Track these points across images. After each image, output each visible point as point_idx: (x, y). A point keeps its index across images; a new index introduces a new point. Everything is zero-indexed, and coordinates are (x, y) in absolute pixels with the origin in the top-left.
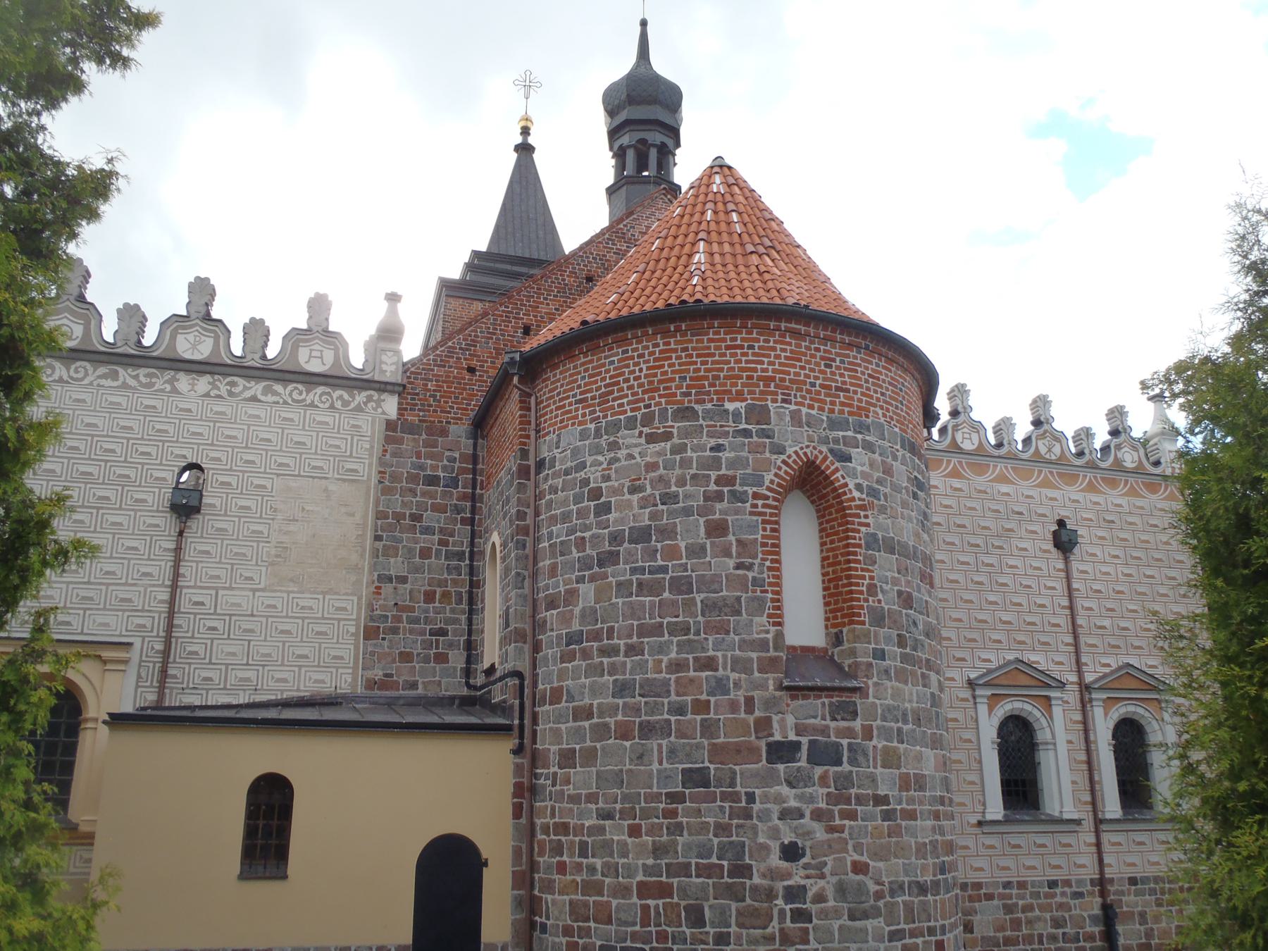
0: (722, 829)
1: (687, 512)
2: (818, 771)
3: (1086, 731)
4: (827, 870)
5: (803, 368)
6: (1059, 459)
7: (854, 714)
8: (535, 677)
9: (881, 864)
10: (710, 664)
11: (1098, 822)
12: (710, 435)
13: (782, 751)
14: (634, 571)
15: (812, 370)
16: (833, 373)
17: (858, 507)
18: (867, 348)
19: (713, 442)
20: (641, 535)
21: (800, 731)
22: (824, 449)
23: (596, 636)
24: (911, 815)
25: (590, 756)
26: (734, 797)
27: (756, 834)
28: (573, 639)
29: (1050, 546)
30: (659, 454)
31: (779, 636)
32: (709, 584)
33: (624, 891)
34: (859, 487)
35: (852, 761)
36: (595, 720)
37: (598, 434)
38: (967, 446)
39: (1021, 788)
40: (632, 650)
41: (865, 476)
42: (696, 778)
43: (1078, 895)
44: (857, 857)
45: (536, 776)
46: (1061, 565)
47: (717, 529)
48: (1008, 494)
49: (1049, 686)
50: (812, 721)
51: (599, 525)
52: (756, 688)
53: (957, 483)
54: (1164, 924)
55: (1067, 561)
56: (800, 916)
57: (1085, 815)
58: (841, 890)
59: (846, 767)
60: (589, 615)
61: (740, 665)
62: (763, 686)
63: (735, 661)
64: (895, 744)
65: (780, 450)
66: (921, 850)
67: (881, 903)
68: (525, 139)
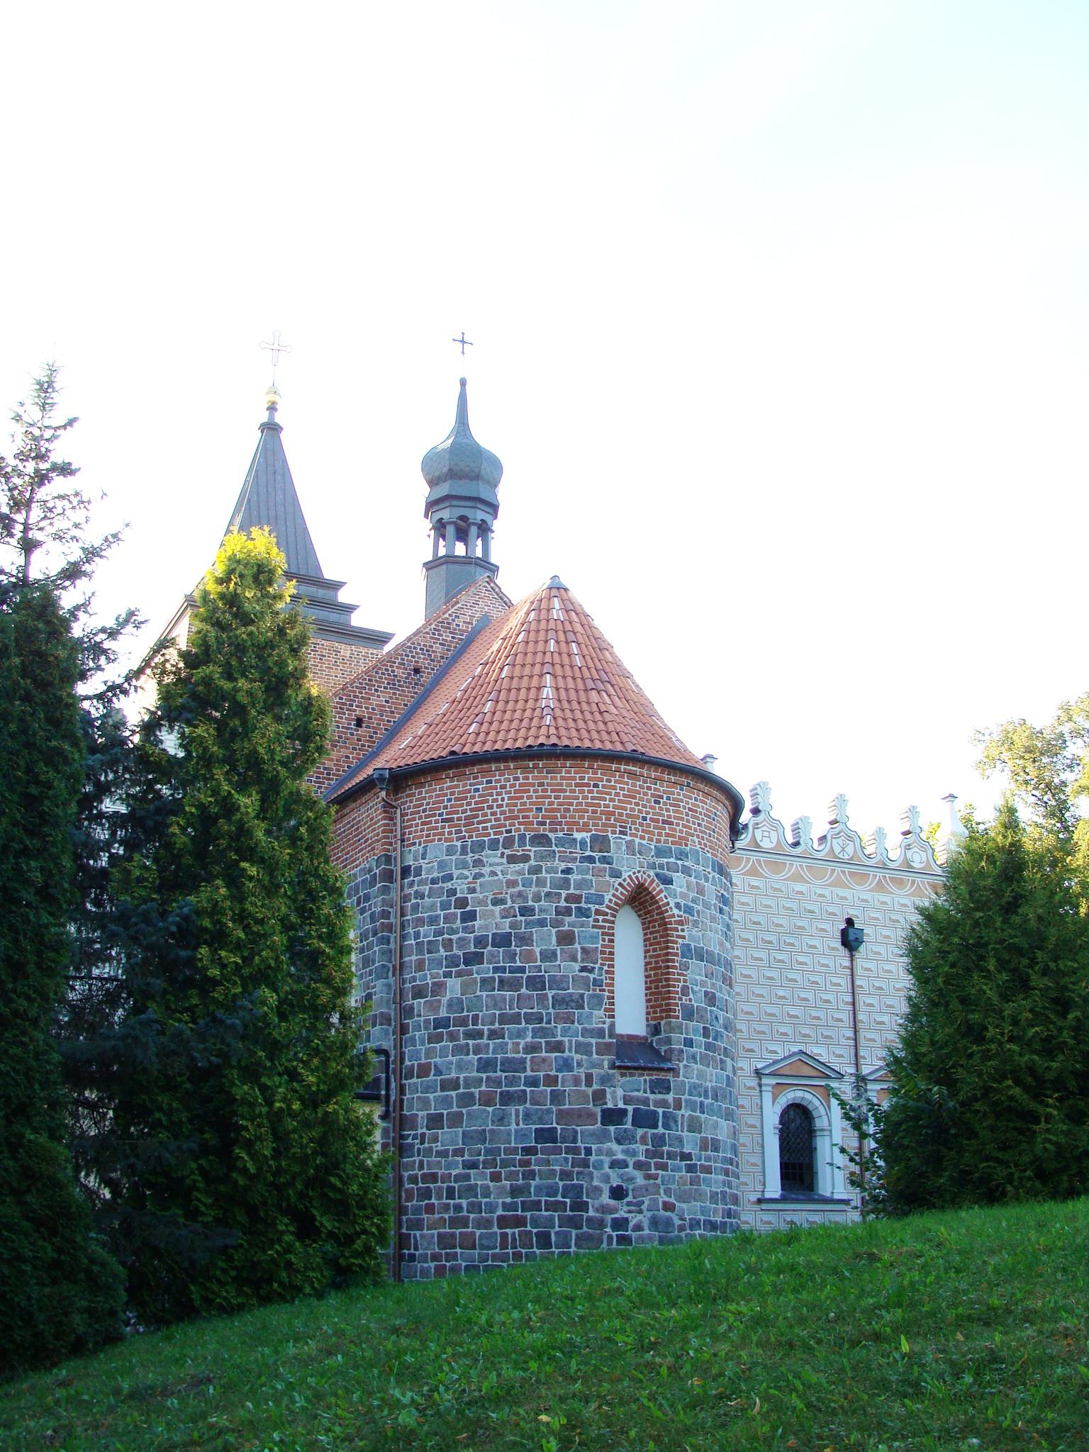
0: (565, 1175)
1: (542, 923)
2: (640, 1132)
4: (644, 1207)
5: (637, 804)
6: (851, 859)
7: (668, 1090)
8: (402, 1054)
9: (684, 1206)
10: (558, 1047)
12: (562, 859)
13: (613, 1116)
14: (496, 970)
15: (645, 806)
16: (661, 809)
18: (688, 785)
19: (563, 866)
20: (502, 940)
21: (627, 1100)
22: (652, 873)
23: (463, 1022)
24: (707, 1170)
25: (456, 1120)
26: (576, 1151)
27: (592, 1179)
28: (439, 1023)
29: (838, 944)
30: (520, 873)
31: (612, 1026)
32: (557, 983)
33: (487, 1224)
34: (678, 906)
35: (666, 1126)
36: (462, 1090)
37: (464, 851)
38: (766, 844)
39: (798, 1172)
40: (493, 1034)
41: (683, 896)
42: (546, 1135)
44: (667, 1199)
45: (402, 1137)
46: (847, 963)
47: (566, 938)
48: (801, 893)
49: (828, 1077)
50: (636, 1094)
51: (465, 930)
52: (594, 1066)
55: (852, 957)
56: (623, 1240)
58: (654, 1223)
59: (661, 1130)
60: (455, 1004)
61: (582, 1048)
62: (600, 1066)
63: (579, 1045)
64: (698, 1114)
65: (616, 874)
66: (714, 1196)
67: (683, 1234)
68: (271, 416)
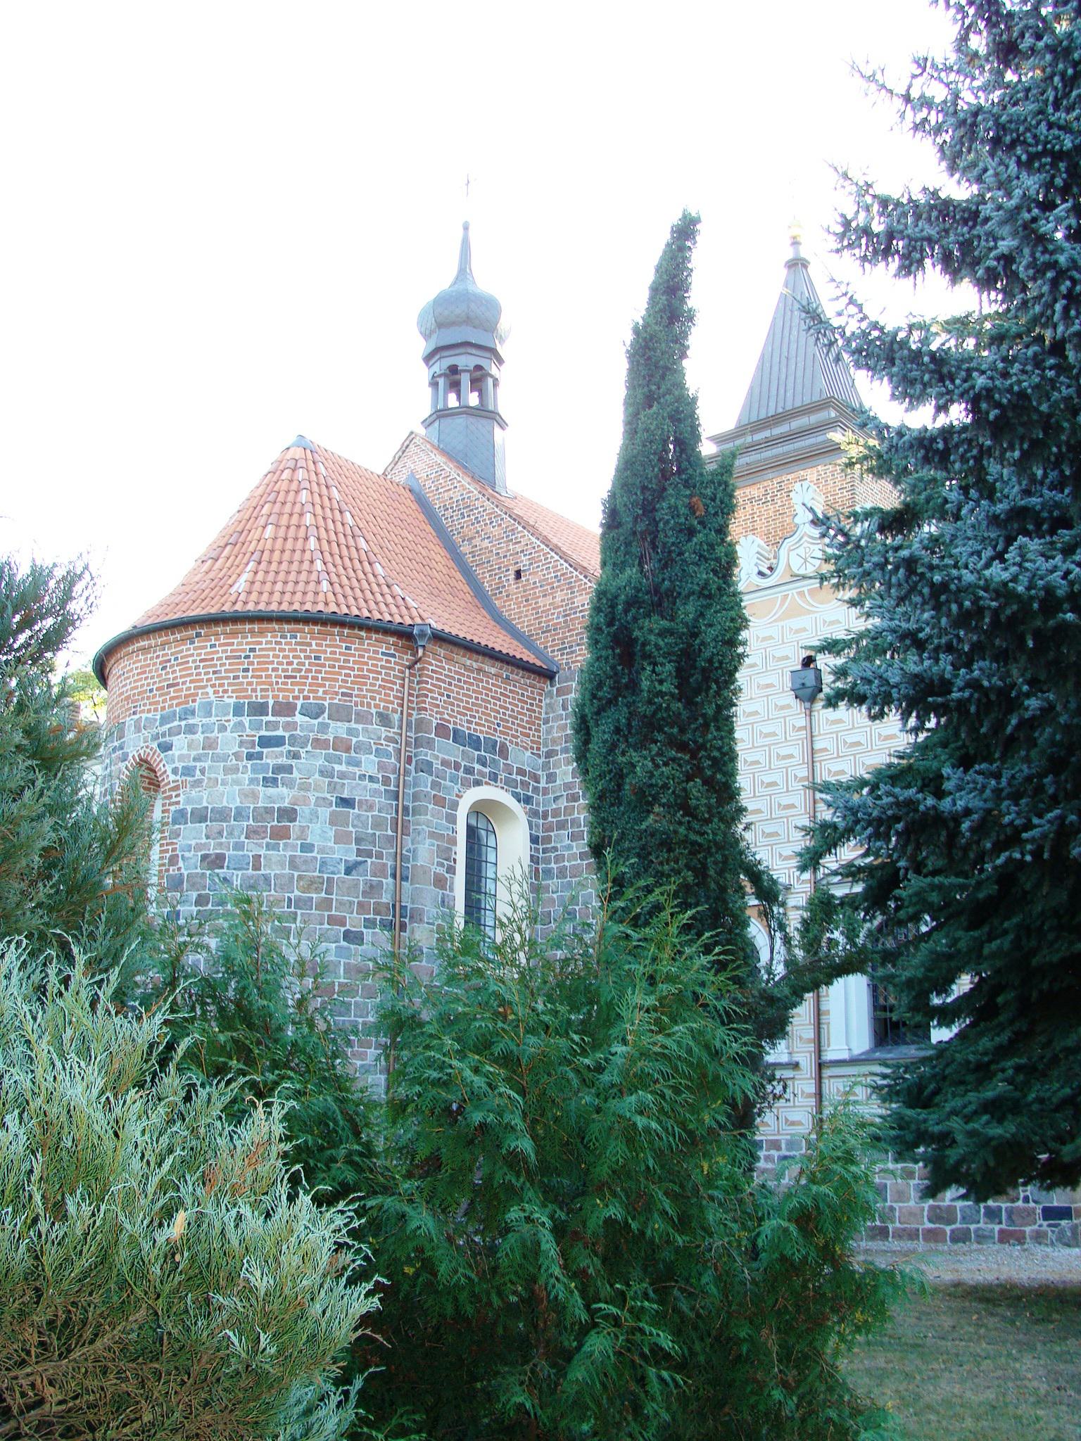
11: (821, 1066)
17: (170, 790)
18: (198, 635)
22: (155, 745)
29: (790, 698)
34: (175, 771)
41: (181, 758)
46: (802, 721)
54: (912, 1203)
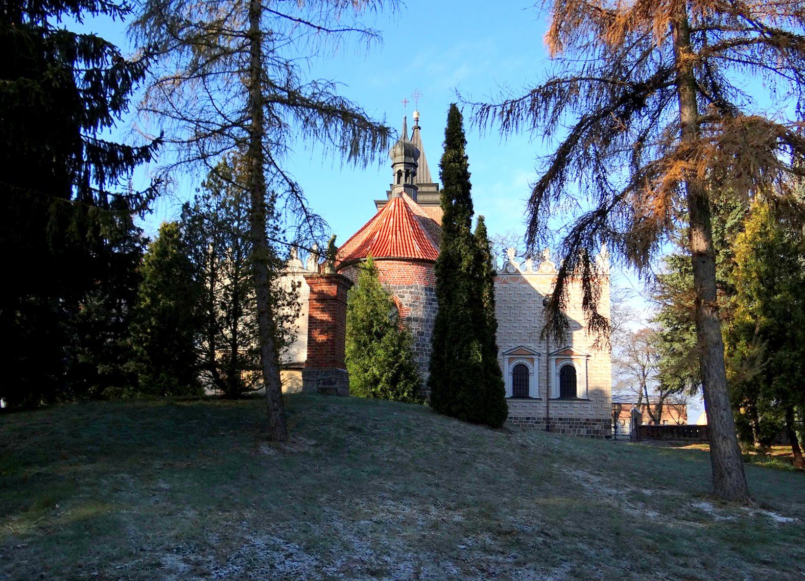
3: (548, 370)
11: (548, 399)
34: (406, 305)
43: (536, 423)
53: (505, 286)
57: (544, 397)
